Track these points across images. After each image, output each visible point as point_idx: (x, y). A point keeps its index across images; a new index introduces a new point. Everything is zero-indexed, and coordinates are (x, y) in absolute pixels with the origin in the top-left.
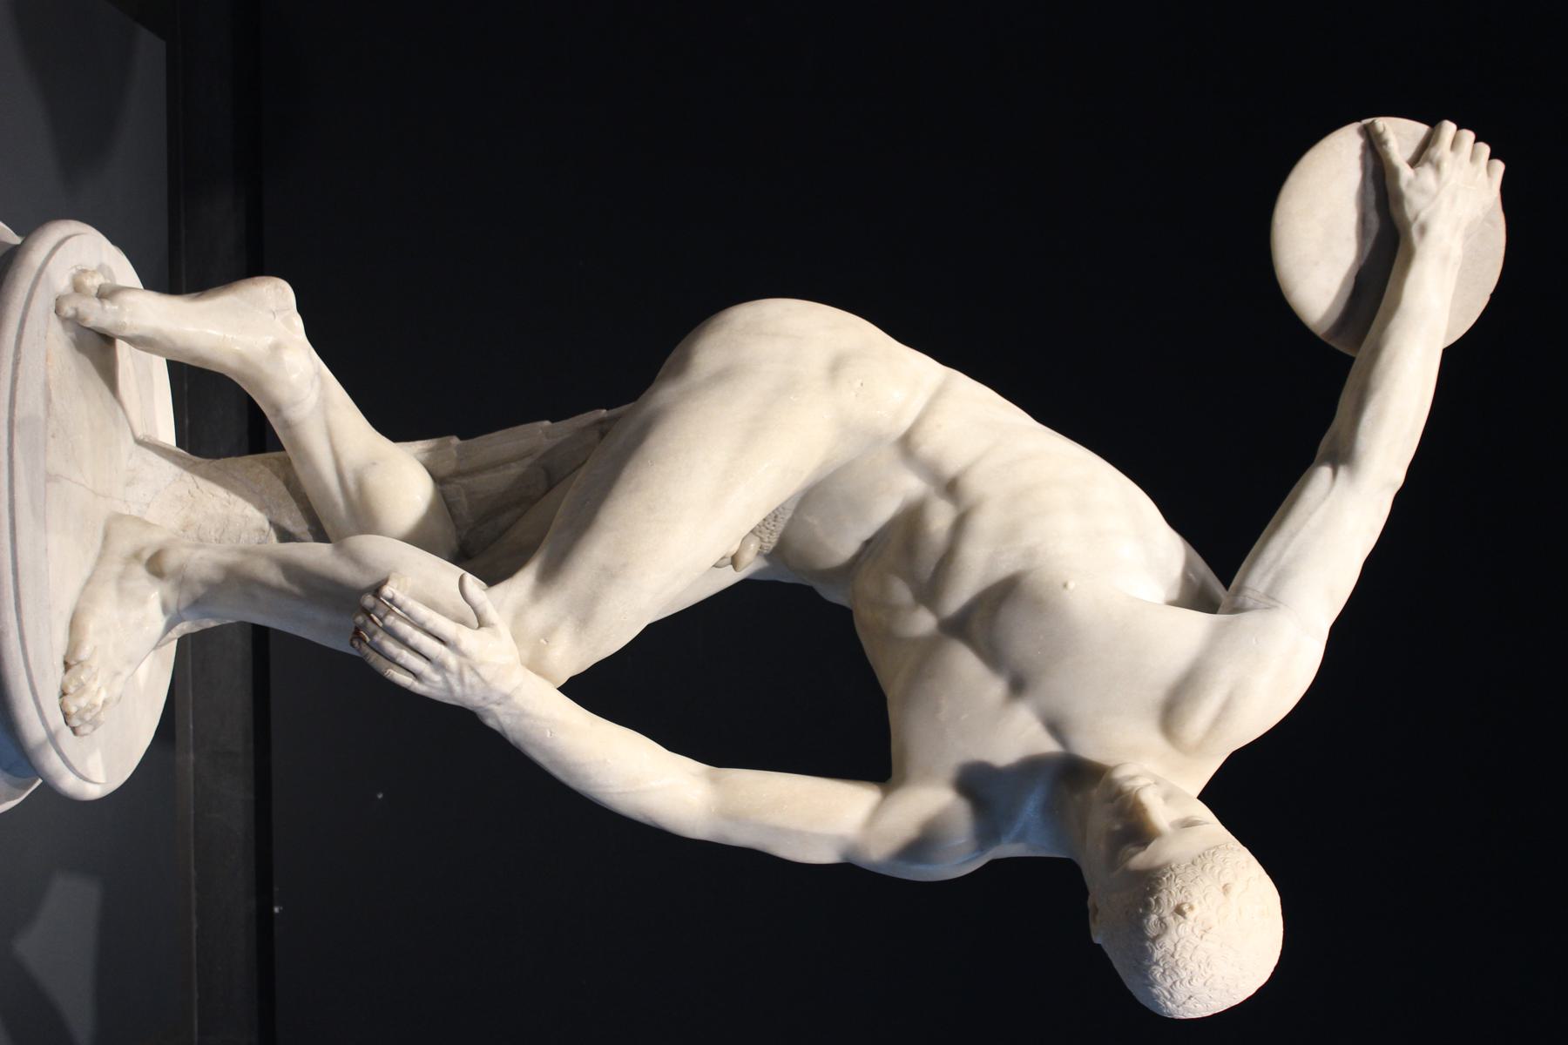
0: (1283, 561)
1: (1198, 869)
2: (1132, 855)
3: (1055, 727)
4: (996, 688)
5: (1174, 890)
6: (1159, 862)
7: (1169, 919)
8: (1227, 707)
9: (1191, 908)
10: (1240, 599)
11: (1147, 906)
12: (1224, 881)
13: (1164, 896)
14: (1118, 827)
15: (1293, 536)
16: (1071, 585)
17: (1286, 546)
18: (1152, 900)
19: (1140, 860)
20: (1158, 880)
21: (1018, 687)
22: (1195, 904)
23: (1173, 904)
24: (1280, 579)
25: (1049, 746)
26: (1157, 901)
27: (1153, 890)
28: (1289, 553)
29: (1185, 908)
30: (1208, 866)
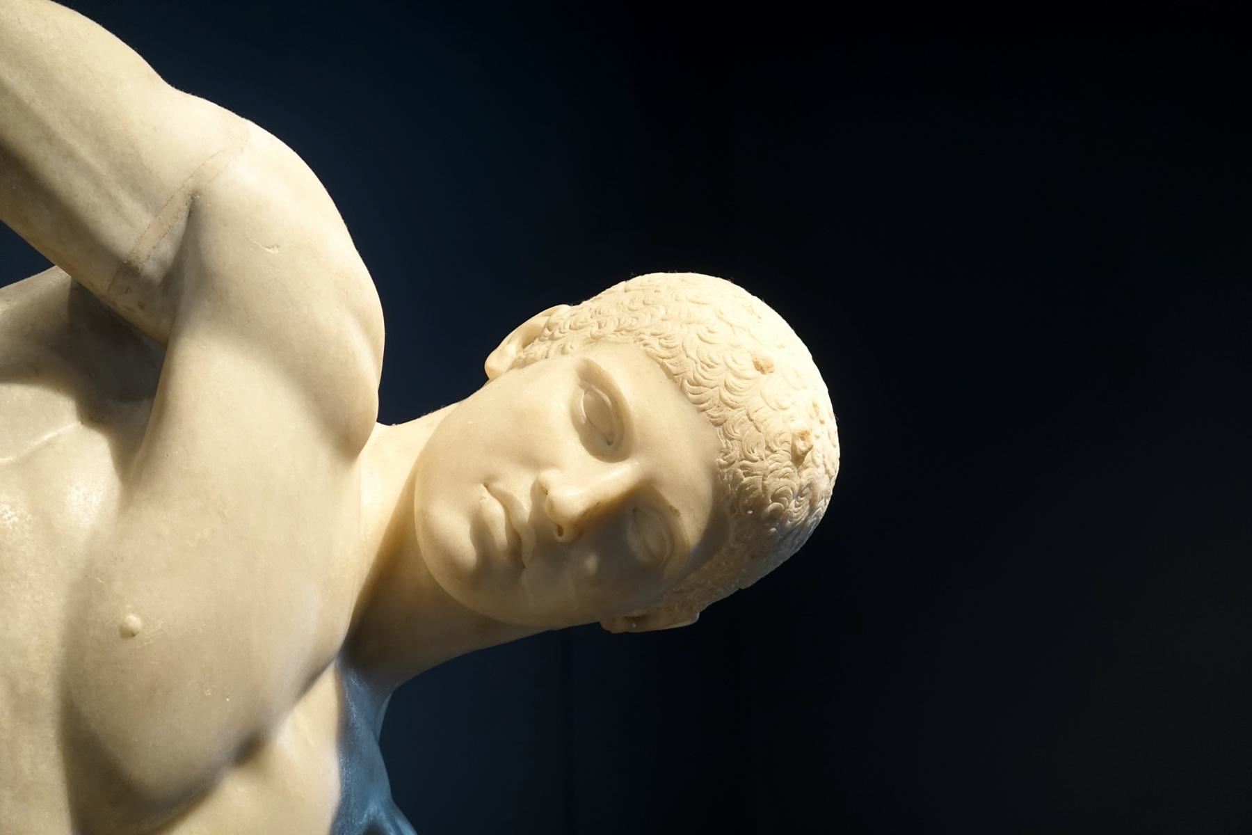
0: (100, 166)
1: (729, 413)
2: (671, 535)
3: (311, 680)
4: (237, 795)
5: (769, 464)
6: (704, 488)
7: (805, 477)
8: (366, 327)
9: (803, 436)
10: (151, 269)
11: (776, 516)
12: (752, 372)
13: (775, 484)
14: (591, 563)
15: (50, 137)
16: (134, 621)
17: (70, 155)
18: (773, 506)
19: (691, 526)
20: (743, 491)
21: (250, 749)
22: (799, 425)
23: (786, 465)
24: (135, 177)
25: (327, 690)
26: (776, 498)
27: (759, 504)
28: (85, 151)
29: (801, 446)
30: (726, 395)
